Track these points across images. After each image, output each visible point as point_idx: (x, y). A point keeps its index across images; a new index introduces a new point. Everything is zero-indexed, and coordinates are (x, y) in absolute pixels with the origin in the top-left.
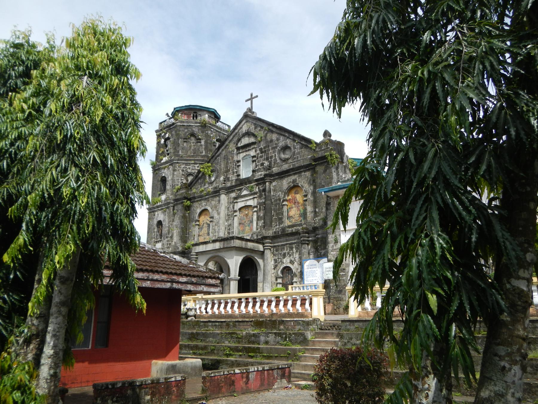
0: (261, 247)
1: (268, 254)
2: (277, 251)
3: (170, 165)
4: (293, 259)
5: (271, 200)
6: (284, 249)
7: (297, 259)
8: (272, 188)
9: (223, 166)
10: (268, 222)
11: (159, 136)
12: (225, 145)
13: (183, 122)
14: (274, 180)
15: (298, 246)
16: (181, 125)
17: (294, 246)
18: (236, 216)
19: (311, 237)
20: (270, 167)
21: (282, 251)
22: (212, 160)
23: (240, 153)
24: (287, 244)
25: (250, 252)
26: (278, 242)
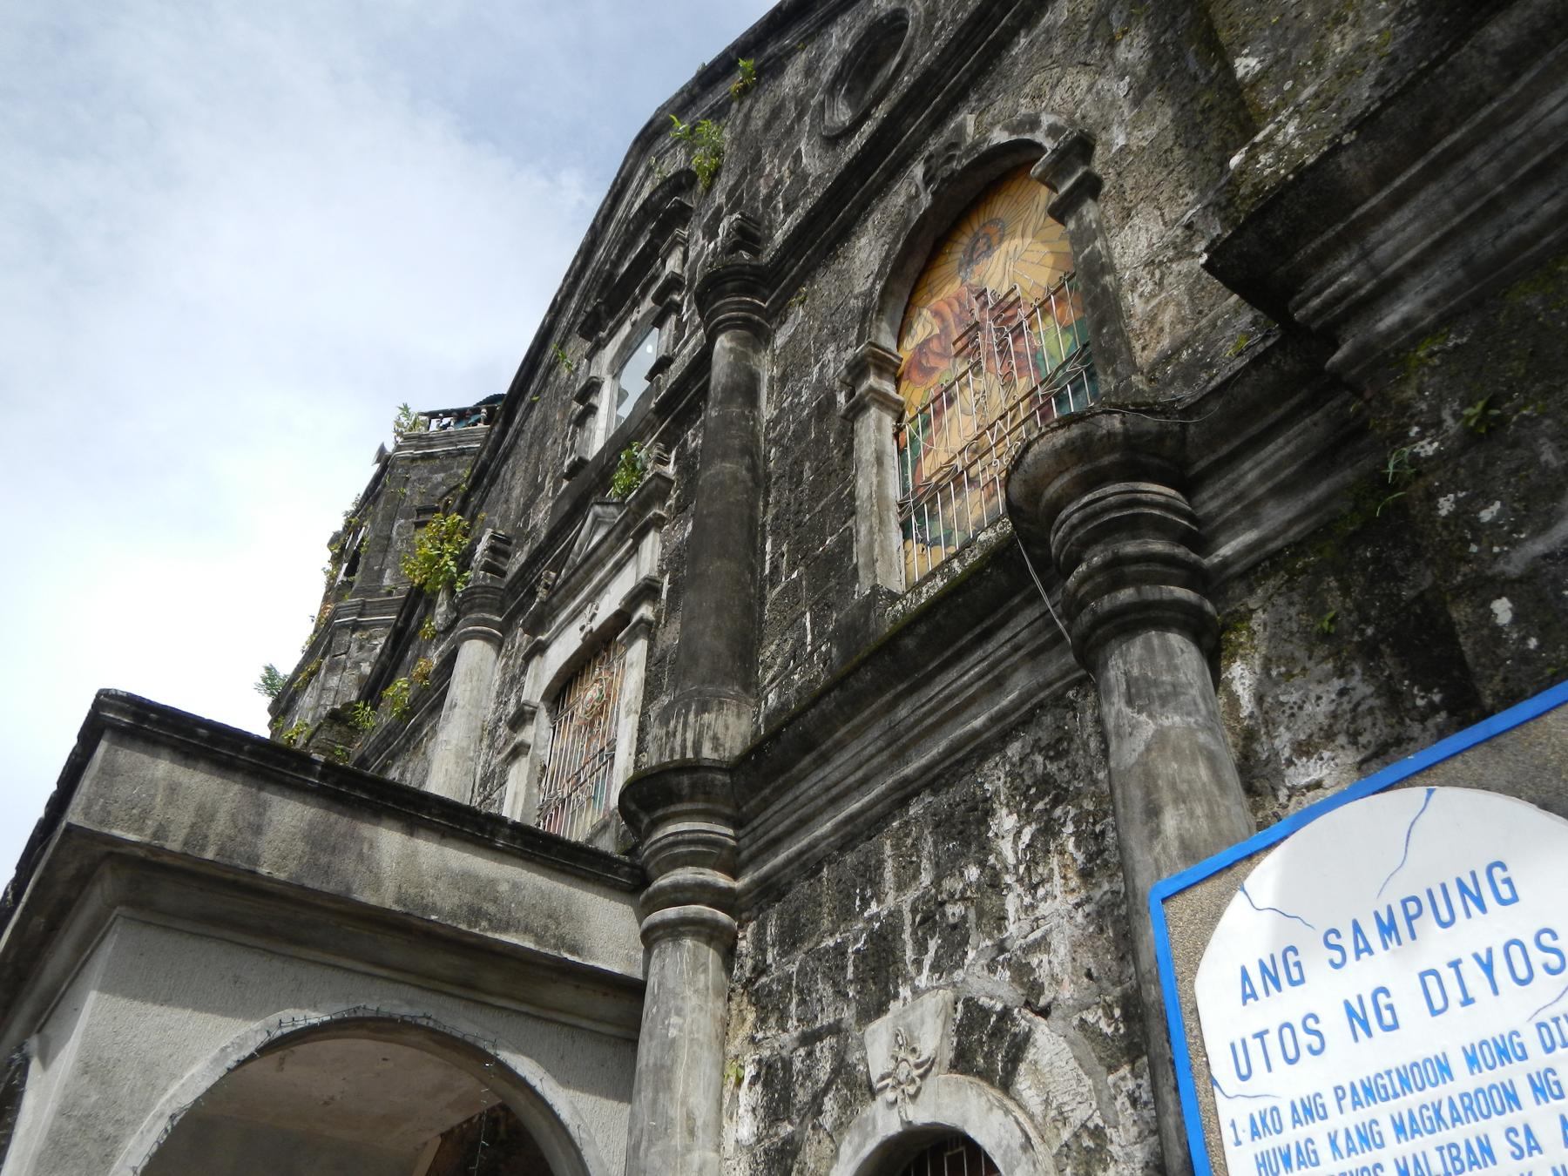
0: (606, 930)
1: (688, 1000)
2: (790, 939)
3: (323, 657)
4: (996, 990)
5: (750, 450)
6: (870, 875)
7: (1059, 968)
8: (767, 369)
9: (516, 492)
10: (712, 642)
11: (336, 560)
12: (541, 371)
13: (430, 440)
14: (779, 313)
15: (1057, 749)
16: (413, 459)
17: (995, 779)
18: (518, 751)
19: (1251, 513)
20: (747, 236)
21: (846, 914)
22: (474, 500)
23: (599, 346)
24: (903, 795)
25: (429, 982)
26: (803, 823)
